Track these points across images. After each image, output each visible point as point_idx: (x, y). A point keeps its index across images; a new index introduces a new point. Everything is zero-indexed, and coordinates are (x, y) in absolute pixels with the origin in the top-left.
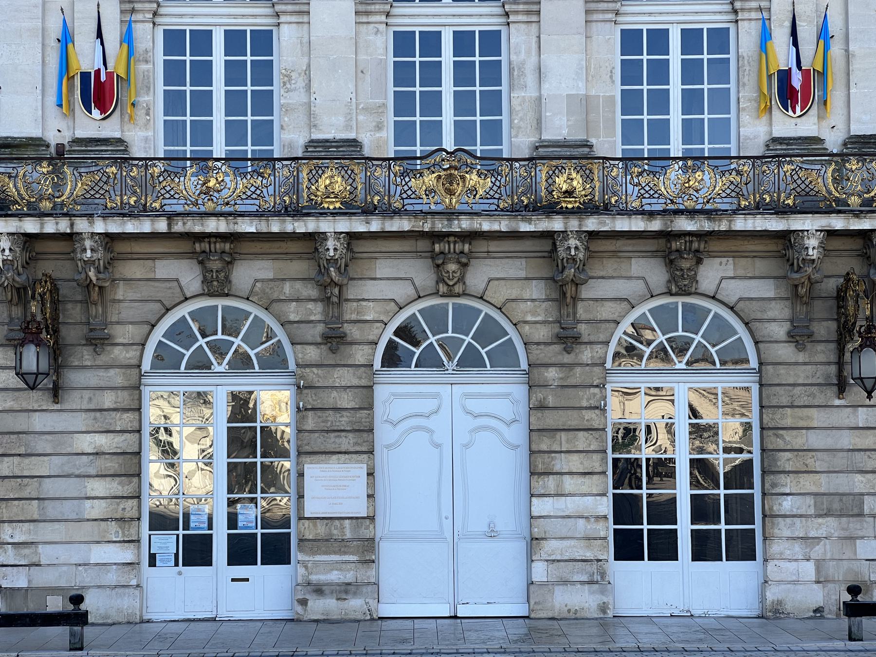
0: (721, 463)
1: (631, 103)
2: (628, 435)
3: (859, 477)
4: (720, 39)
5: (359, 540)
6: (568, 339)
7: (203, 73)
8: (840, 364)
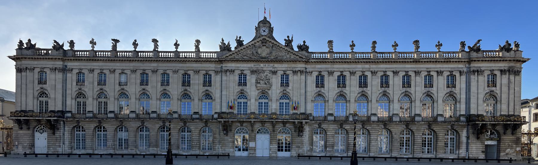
0: (288, 143)
1: (280, 109)
2: (279, 140)
4: (288, 103)
5: (254, 149)
7: (241, 106)
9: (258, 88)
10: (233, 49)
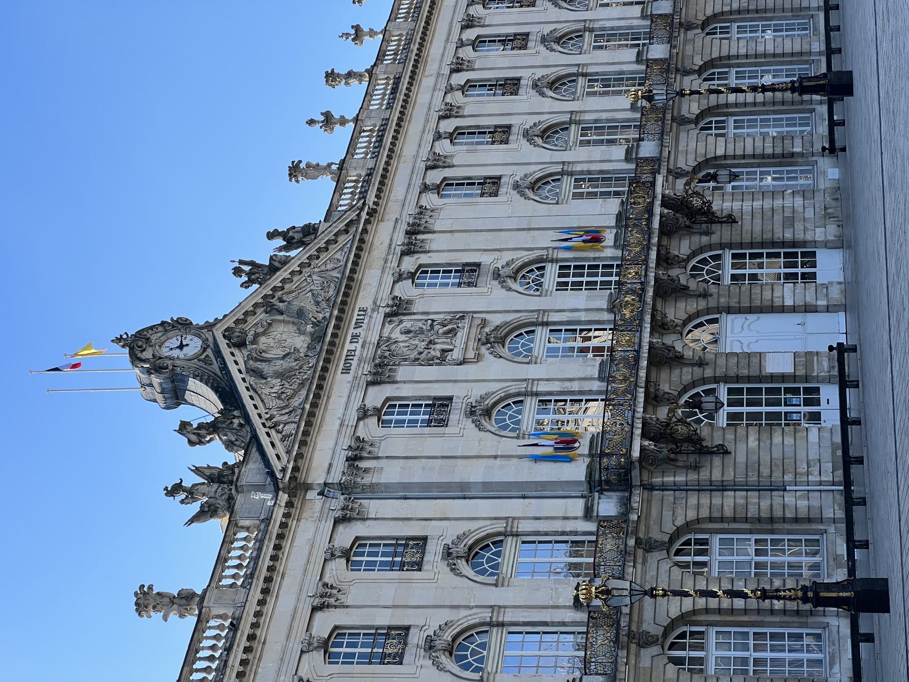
3: (775, 217)
4: (564, 270)
6: (705, 295)
8: (722, 222)
9: (471, 354)
10: (233, 458)
